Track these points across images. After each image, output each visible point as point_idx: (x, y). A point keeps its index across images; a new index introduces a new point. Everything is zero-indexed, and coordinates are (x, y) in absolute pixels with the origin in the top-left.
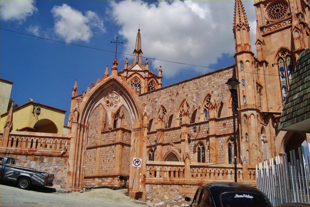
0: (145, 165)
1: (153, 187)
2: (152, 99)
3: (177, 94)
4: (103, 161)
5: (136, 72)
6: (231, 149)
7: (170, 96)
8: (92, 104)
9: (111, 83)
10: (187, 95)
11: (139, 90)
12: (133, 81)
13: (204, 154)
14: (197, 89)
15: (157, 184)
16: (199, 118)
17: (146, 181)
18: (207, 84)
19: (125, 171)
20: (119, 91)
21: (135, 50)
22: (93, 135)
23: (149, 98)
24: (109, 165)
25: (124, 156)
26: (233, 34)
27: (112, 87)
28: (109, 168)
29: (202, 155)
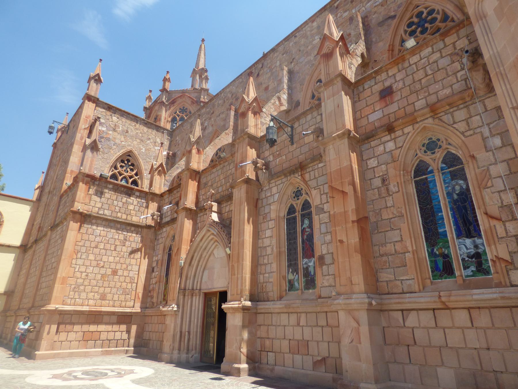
6: (431, 186)
13: (311, 226)
29: (303, 231)
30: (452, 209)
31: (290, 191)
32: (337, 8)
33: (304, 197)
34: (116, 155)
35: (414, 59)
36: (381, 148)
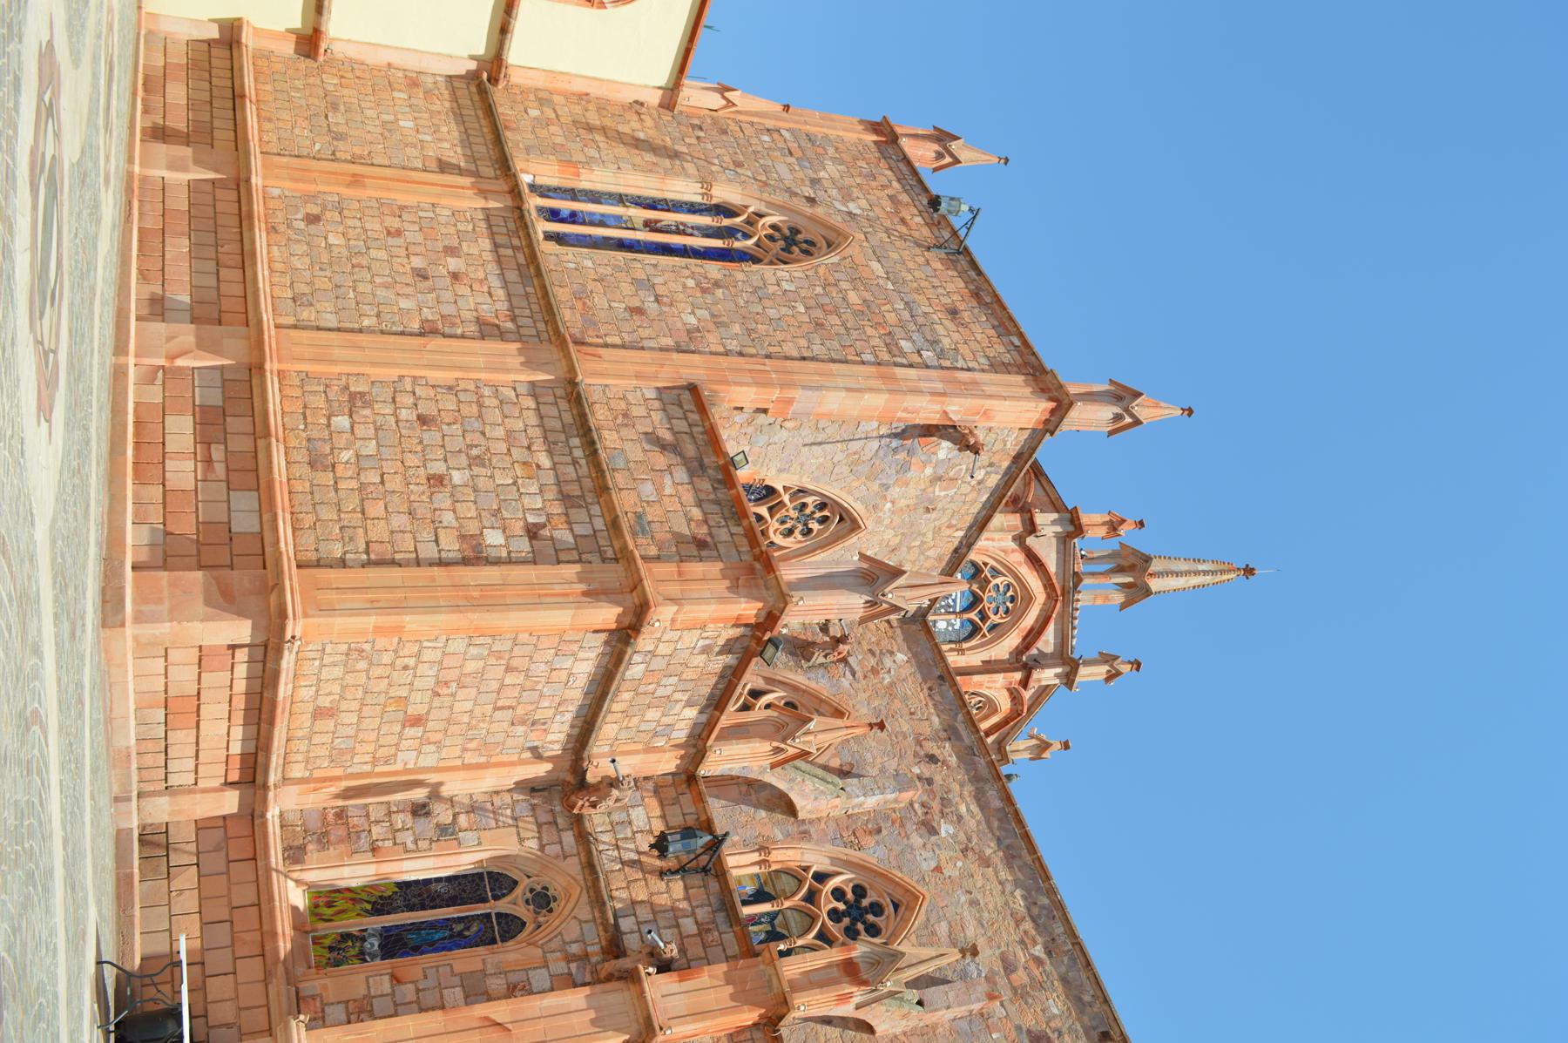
2: (938, 779)
4: (423, 420)
12: (998, 581)
19: (338, 672)
22: (651, 306)
23: (937, 752)
24: (394, 483)
25: (498, 655)
28: (362, 487)
34: (844, 495)
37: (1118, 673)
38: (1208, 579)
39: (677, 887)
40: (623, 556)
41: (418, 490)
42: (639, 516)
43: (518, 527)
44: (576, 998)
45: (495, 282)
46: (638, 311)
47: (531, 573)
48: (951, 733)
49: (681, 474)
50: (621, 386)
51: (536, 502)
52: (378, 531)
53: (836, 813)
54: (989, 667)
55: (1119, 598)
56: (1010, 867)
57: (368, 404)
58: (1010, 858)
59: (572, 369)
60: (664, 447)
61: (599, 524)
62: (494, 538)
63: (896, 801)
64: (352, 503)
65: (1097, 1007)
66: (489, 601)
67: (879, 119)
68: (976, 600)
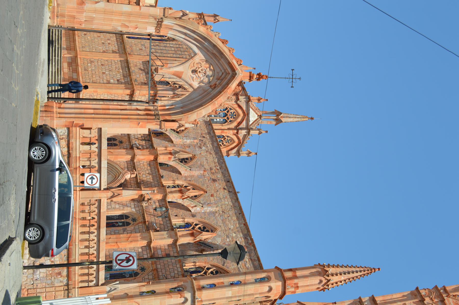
0: (100, 127)
1: (64, 140)
3: (214, 180)
4: (102, 65)
5: (246, 115)
7: (211, 169)
8: (195, 40)
9: (229, 70)
10: (212, 195)
11: (218, 120)
12: (232, 111)
13: (119, 226)
14: (223, 212)
15: (68, 147)
16: (176, 216)
17: (74, 129)
18: (232, 227)
20: (217, 83)
21: (281, 113)
22: (144, 48)
24: (97, 73)
26: (313, 265)
27: (223, 71)
29: (117, 223)
30: (119, 273)
31: (136, 216)
32: (246, 238)
33: (132, 223)
35: (178, 266)
36: (145, 253)
37: (261, 133)
38: (299, 119)
39: (144, 142)
40: (132, 84)
41: (101, 74)
42: (136, 79)
43: (116, 80)
44: (124, 150)
45: (116, 45)
46: (141, 49)
47: (117, 85)
48: (209, 133)
49: (144, 74)
50: (136, 62)
51: (119, 76)
52: (94, 79)
53: (181, 143)
54: (229, 129)
55: (274, 123)
56: (216, 155)
57: (93, 62)
58: (216, 154)
59: (127, 58)
60: (142, 70)
61: (129, 80)
62: (112, 81)
63: (193, 142)
64: (91, 75)
65: (228, 177)
66: (110, 88)
67: (201, 13)
68: (226, 115)
